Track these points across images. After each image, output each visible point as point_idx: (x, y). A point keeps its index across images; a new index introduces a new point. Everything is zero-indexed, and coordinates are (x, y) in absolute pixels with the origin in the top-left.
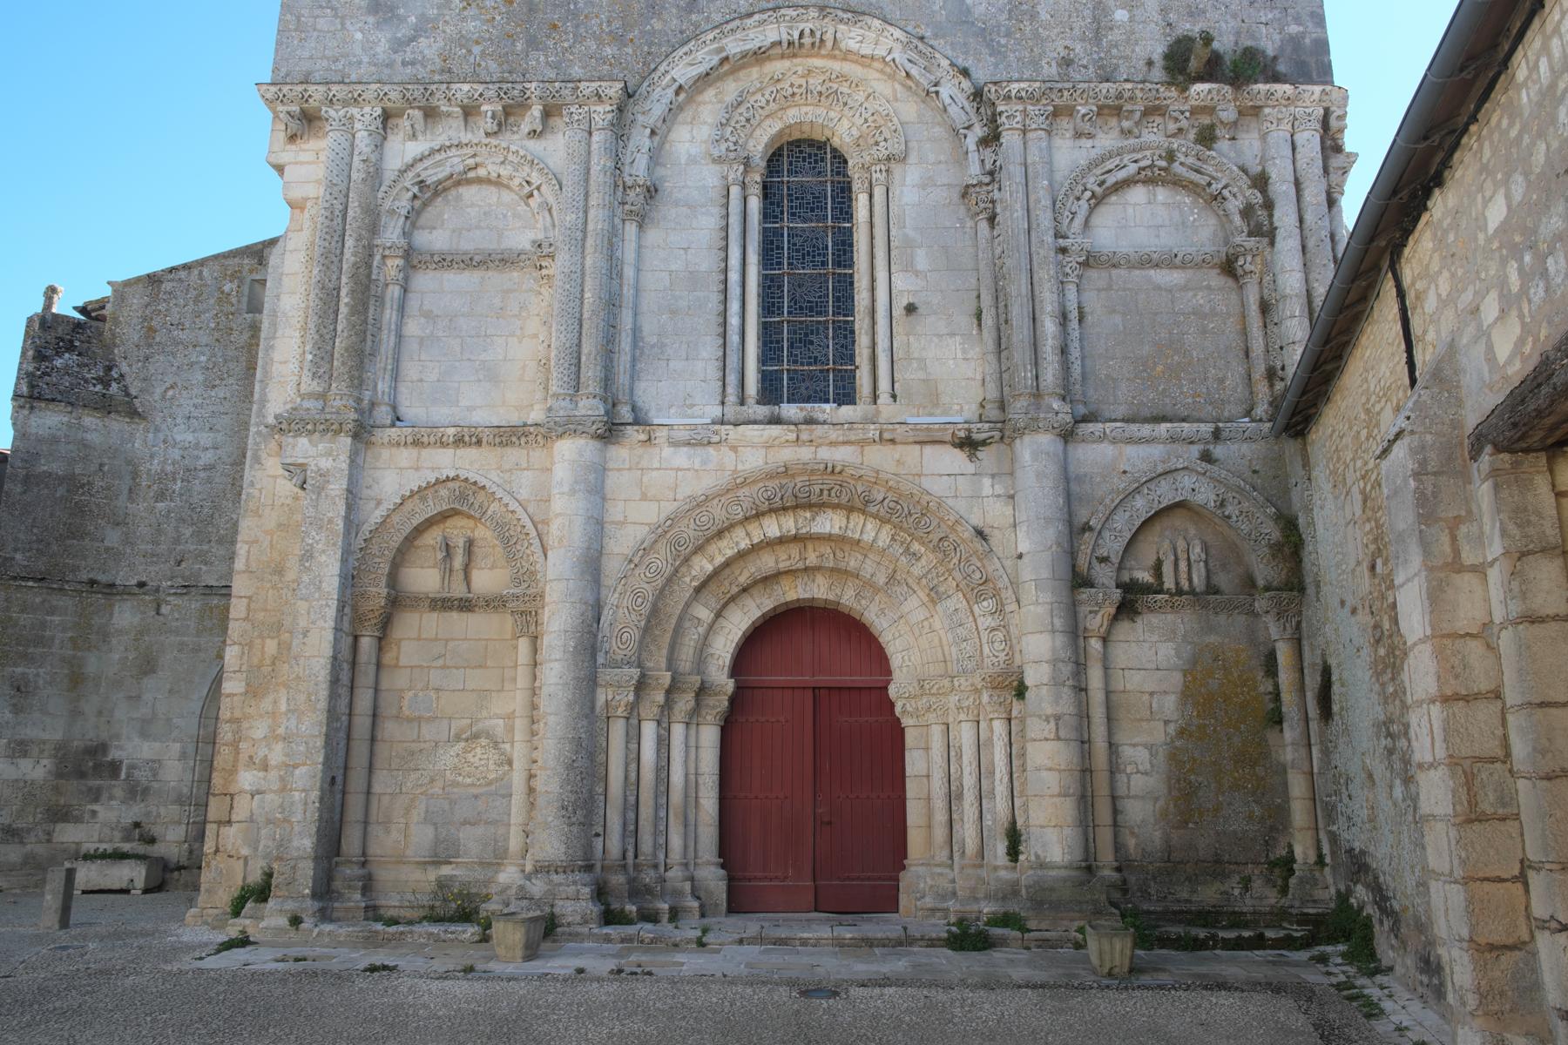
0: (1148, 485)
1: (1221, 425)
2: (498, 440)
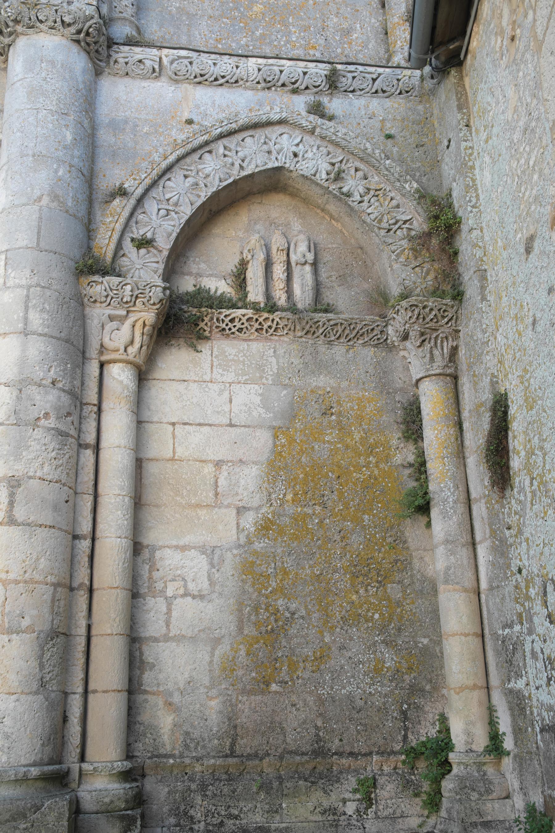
0: (225, 141)
1: (339, 67)
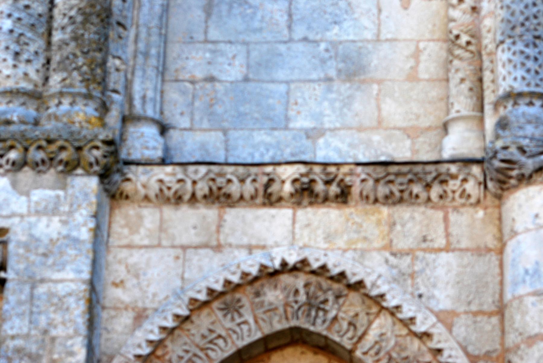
2: (382, 190)
